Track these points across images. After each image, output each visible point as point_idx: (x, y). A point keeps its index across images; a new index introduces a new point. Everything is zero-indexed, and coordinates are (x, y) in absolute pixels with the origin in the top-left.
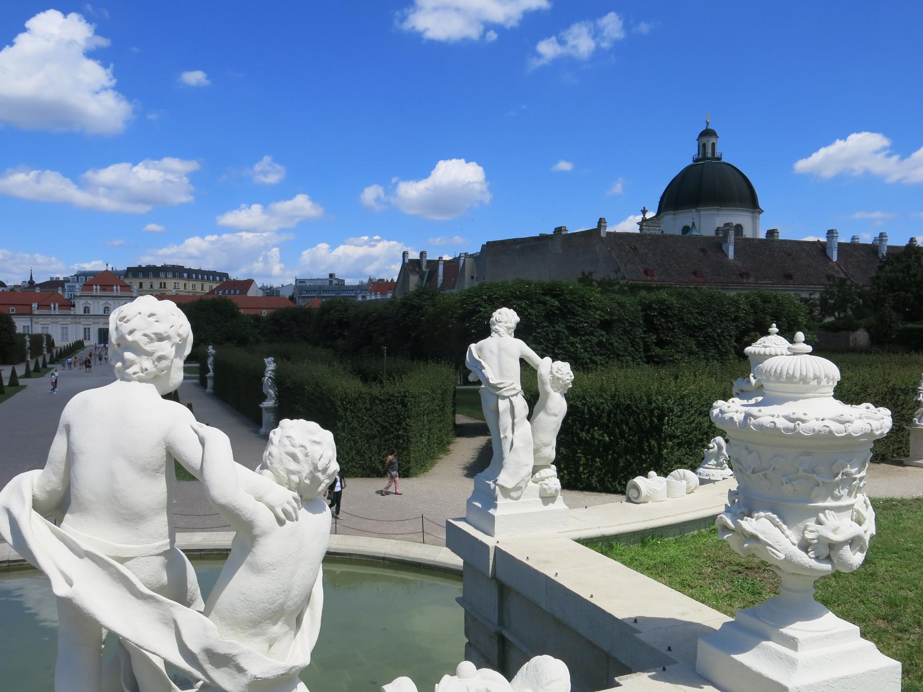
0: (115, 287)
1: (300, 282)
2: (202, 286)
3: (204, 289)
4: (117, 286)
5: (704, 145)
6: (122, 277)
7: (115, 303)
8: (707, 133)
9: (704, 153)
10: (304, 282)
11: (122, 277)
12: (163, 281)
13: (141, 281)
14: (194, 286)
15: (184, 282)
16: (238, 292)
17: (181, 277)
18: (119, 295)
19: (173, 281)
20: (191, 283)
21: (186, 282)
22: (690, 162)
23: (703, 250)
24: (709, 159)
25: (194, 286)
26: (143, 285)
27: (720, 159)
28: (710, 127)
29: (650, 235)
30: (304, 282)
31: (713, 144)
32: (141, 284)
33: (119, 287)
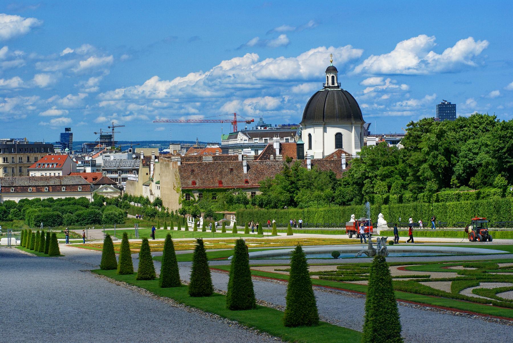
1: (105, 156)
2: (28, 158)
3: (30, 160)
5: (328, 77)
8: (331, 70)
9: (328, 83)
10: (109, 156)
14: (20, 158)
16: (55, 165)
17: (10, 152)
20: (18, 156)
21: (14, 156)
23: (232, 170)
24: (329, 87)
25: (20, 158)
27: (338, 87)
28: (334, 64)
30: (109, 156)
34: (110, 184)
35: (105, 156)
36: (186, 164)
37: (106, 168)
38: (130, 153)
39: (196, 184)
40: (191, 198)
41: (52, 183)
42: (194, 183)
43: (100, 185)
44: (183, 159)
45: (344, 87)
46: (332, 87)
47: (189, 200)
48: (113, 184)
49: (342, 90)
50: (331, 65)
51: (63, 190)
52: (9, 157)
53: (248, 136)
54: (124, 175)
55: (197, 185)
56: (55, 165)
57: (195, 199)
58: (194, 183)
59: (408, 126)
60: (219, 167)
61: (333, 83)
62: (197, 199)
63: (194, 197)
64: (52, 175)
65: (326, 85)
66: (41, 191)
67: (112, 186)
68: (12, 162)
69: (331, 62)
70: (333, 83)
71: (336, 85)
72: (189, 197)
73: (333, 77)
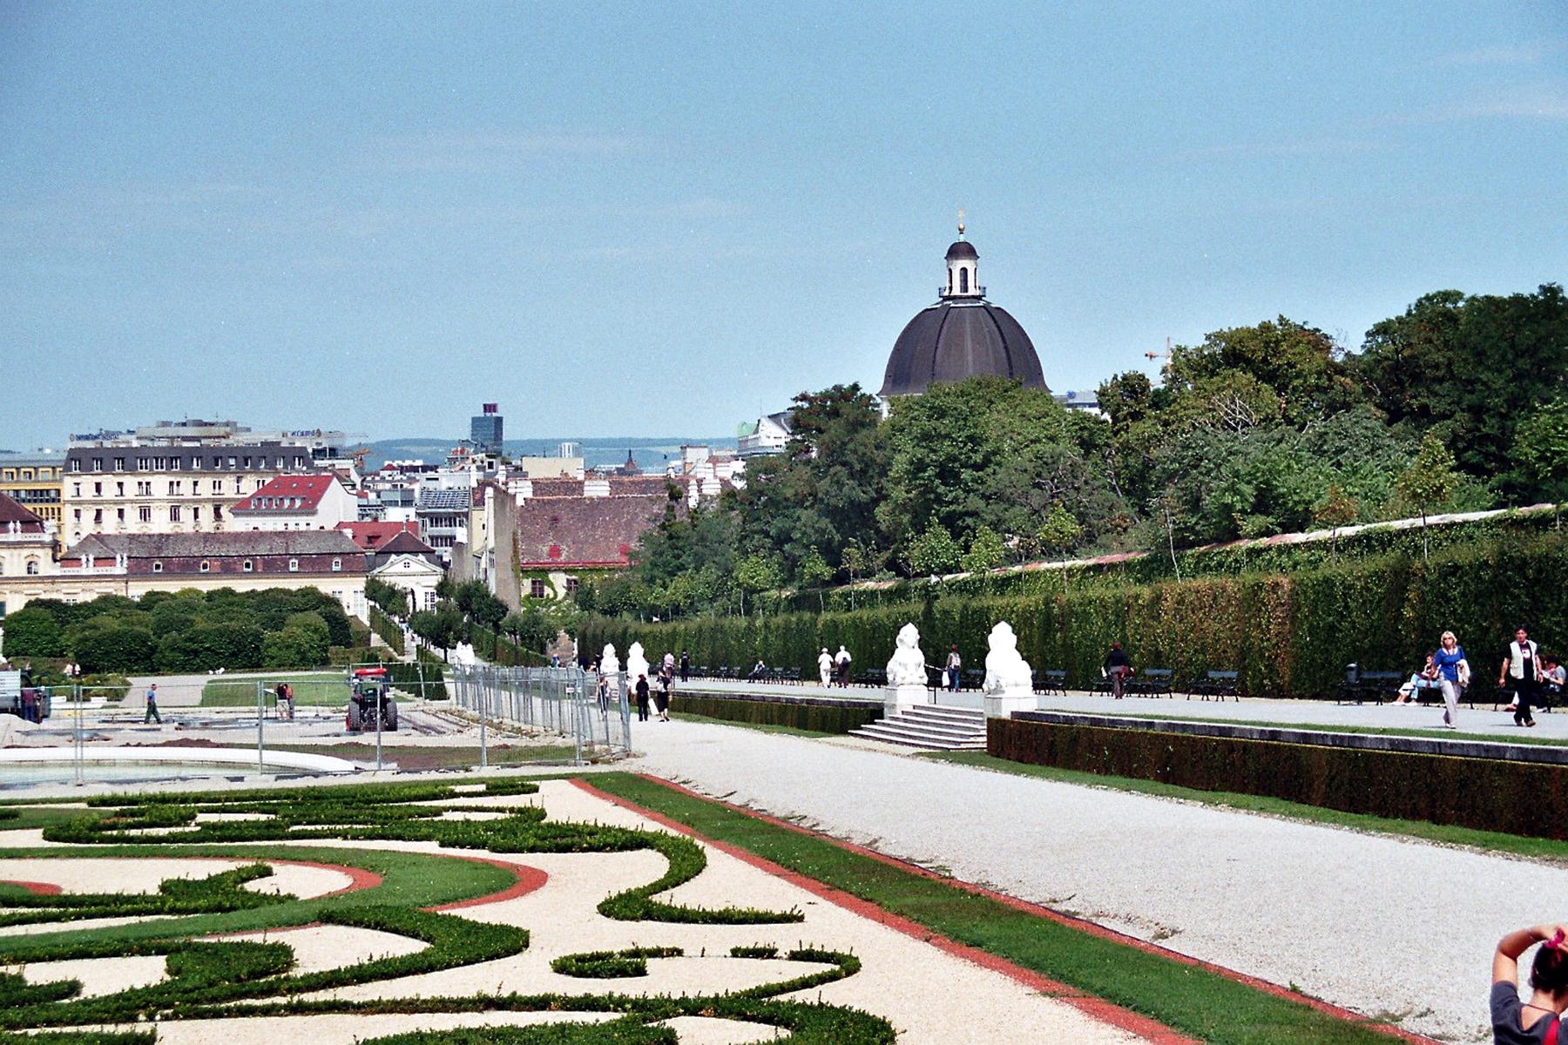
0: (11, 525)
1: (428, 479)
4: (15, 522)
6: (58, 469)
7: (12, 555)
9: (951, 288)
10: (437, 479)
11: (58, 469)
12: (144, 479)
13: (98, 479)
15: (191, 480)
16: (298, 503)
17: (187, 470)
18: (19, 539)
19: (167, 479)
22: (932, 300)
24: (954, 298)
26: (103, 487)
27: (979, 298)
29: (591, 499)
30: (437, 479)
31: (964, 271)
32: (98, 487)
33: (18, 524)
34: (416, 553)
35: (428, 479)
36: (538, 501)
37: (428, 510)
38: (491, 470)
39: (559, 555)
40: (548, 591)
41: (263, 549)
42: (555, 552)
43: (391, 553)
44: (559, 488)
45: (994, 299)
46: (960, 297)
47: (542, 596)
48: (422, 552)
49: (987, 307)
50: (962, 238)
51: (292, 569)
52: (187, 482)
53: (784, 429)
54: (444, 530)
55: (562, 558)
56: (298, 503)
57: (556, 595)
58: (555, 552)
59: (796, 399)
60: (625, 510)
61: (965, 288)
62: (562, 593)
63: (551, 585)
64: (303, 527)
65: (946, 293)
66: (235, 569)
67: (421, 557)
68: (194, 494)
69: (961, 231)
70: (965, 288)
71: (972, 291)
72: (542, 590)
73: (964, 271)
